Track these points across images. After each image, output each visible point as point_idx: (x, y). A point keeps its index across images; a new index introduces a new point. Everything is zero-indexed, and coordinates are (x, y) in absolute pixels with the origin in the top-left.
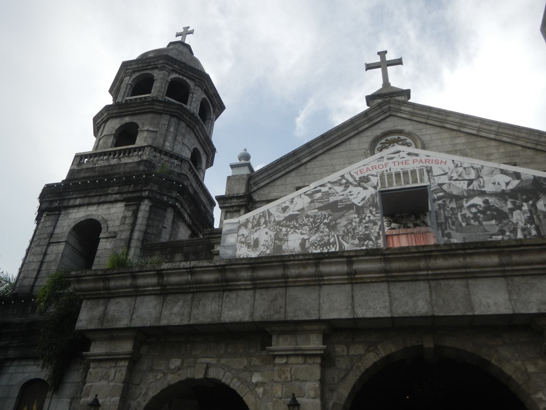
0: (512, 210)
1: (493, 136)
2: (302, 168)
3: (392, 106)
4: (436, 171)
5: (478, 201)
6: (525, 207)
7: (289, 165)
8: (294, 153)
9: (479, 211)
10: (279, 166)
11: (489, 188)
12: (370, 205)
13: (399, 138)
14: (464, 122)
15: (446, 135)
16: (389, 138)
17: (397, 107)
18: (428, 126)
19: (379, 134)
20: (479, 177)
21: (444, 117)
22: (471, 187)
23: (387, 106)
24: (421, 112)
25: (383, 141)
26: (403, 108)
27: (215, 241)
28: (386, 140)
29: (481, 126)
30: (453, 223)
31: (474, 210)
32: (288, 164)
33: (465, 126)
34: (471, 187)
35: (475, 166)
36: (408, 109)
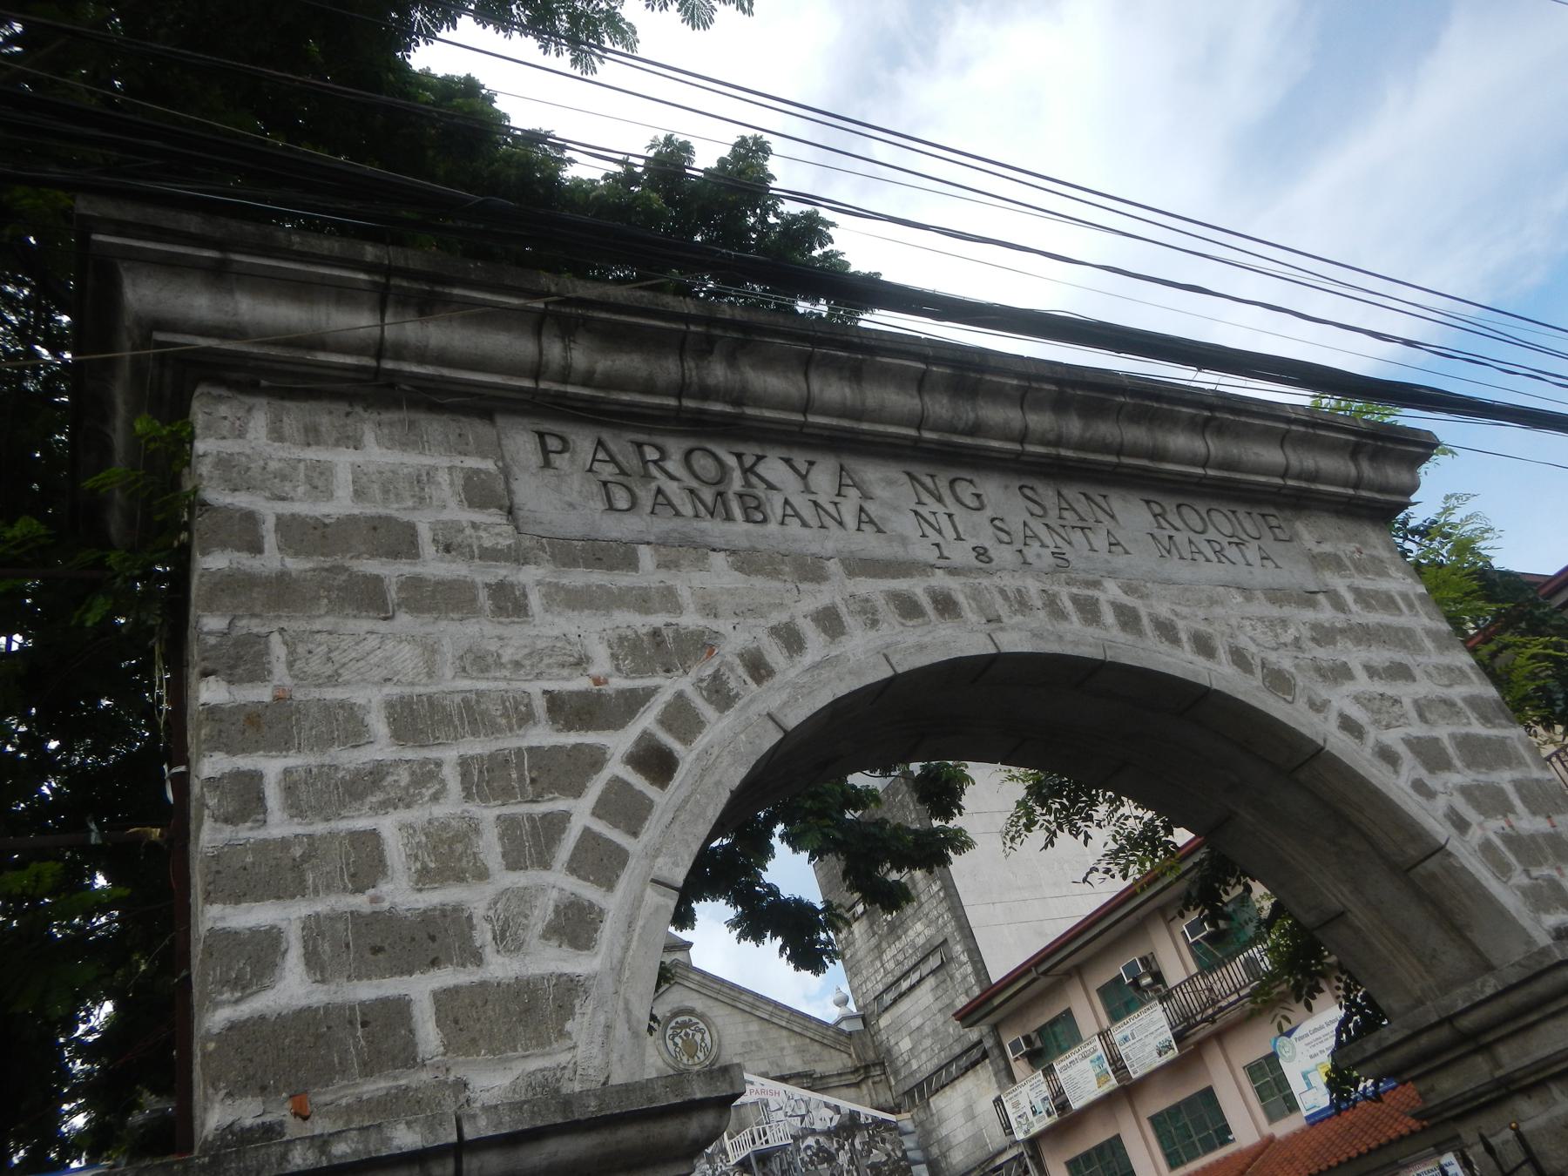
0: (837, 1150)
1: (784, 1024)
3: (679, 970)
4: (773, 1106)
5: (810, 1141)
6: (847, 1147)
9: (814, 1154)
11: (818, 1126)
12: (720, 1152)
13: (690, 1020)
14: (757, 1003)
15: (739, 1017)
16: (679, 1019)
18: (718, 1004)
19: (668, 1015)
20: (808, 1112)
21: (737, 995)
22: (804, 1125)
24: (712, 985)
25: (673, 1024)
28: (677, 1023)
30: (795, 1169)
31: (809, 1153)
33: (757, 1008)
34: (804, 1125)
35: (805, 1099)
36: (697, 978)
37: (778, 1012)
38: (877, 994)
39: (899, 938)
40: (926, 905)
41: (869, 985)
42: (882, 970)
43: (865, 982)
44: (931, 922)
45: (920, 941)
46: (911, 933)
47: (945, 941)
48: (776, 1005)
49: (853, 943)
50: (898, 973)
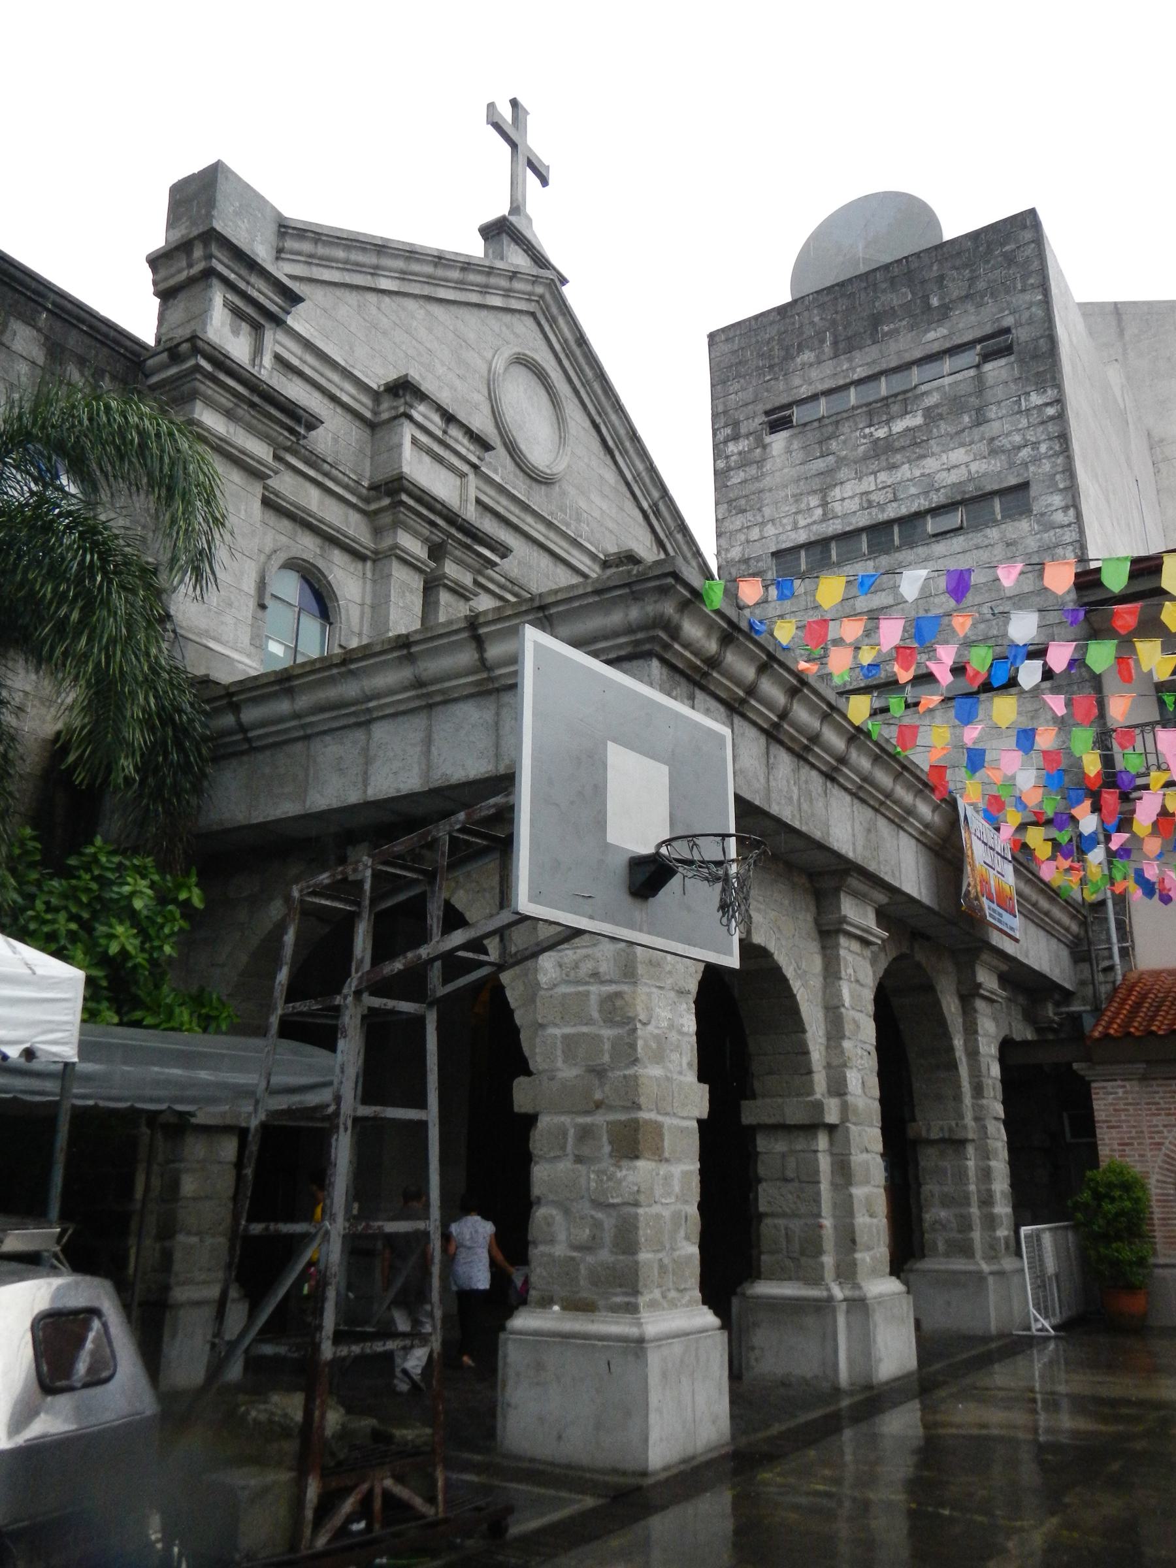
1: (645, 505)
2: (372, 298)
3: (548, 297)
7: (357, 268)
8: (381, 248)
10: (341, 254)
14: (628, 444)
17: (554, 310)
18: (576, 401)
23: (540, 290)
26: (561, 321)
27: (210, 392)
29: (644, 474)
32: (357, 264)
33: (624, 452)
37: (647, 480)
38: (784, 546)
39: (893, 467)
40: (996, 425)
41: (770, 530)
42: (819, 511)
43: (763, 524)
44: (994, 452)
45: (953, 477)
46: (931, 464)
47: (1024, 486)
48: (652, 469)
49: (760, 463)
50: (862, 520)
